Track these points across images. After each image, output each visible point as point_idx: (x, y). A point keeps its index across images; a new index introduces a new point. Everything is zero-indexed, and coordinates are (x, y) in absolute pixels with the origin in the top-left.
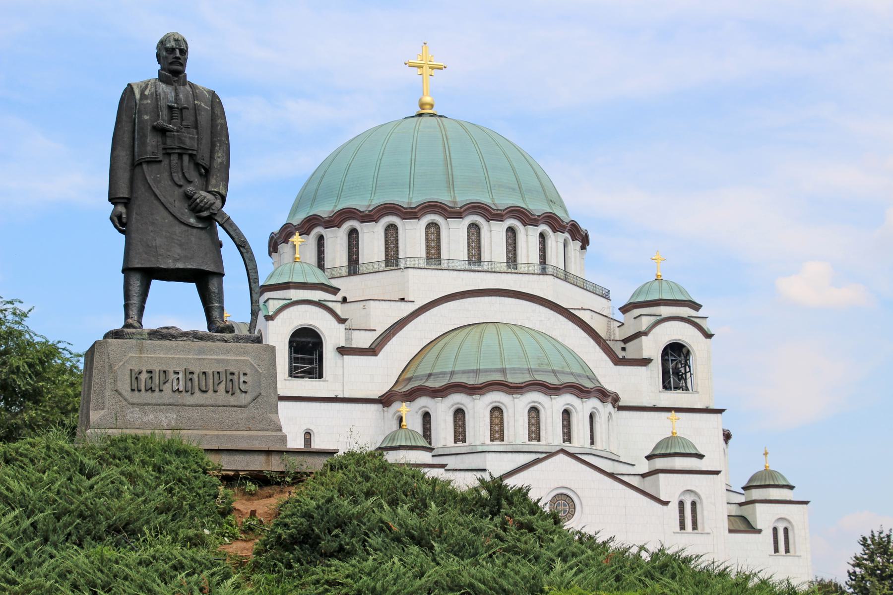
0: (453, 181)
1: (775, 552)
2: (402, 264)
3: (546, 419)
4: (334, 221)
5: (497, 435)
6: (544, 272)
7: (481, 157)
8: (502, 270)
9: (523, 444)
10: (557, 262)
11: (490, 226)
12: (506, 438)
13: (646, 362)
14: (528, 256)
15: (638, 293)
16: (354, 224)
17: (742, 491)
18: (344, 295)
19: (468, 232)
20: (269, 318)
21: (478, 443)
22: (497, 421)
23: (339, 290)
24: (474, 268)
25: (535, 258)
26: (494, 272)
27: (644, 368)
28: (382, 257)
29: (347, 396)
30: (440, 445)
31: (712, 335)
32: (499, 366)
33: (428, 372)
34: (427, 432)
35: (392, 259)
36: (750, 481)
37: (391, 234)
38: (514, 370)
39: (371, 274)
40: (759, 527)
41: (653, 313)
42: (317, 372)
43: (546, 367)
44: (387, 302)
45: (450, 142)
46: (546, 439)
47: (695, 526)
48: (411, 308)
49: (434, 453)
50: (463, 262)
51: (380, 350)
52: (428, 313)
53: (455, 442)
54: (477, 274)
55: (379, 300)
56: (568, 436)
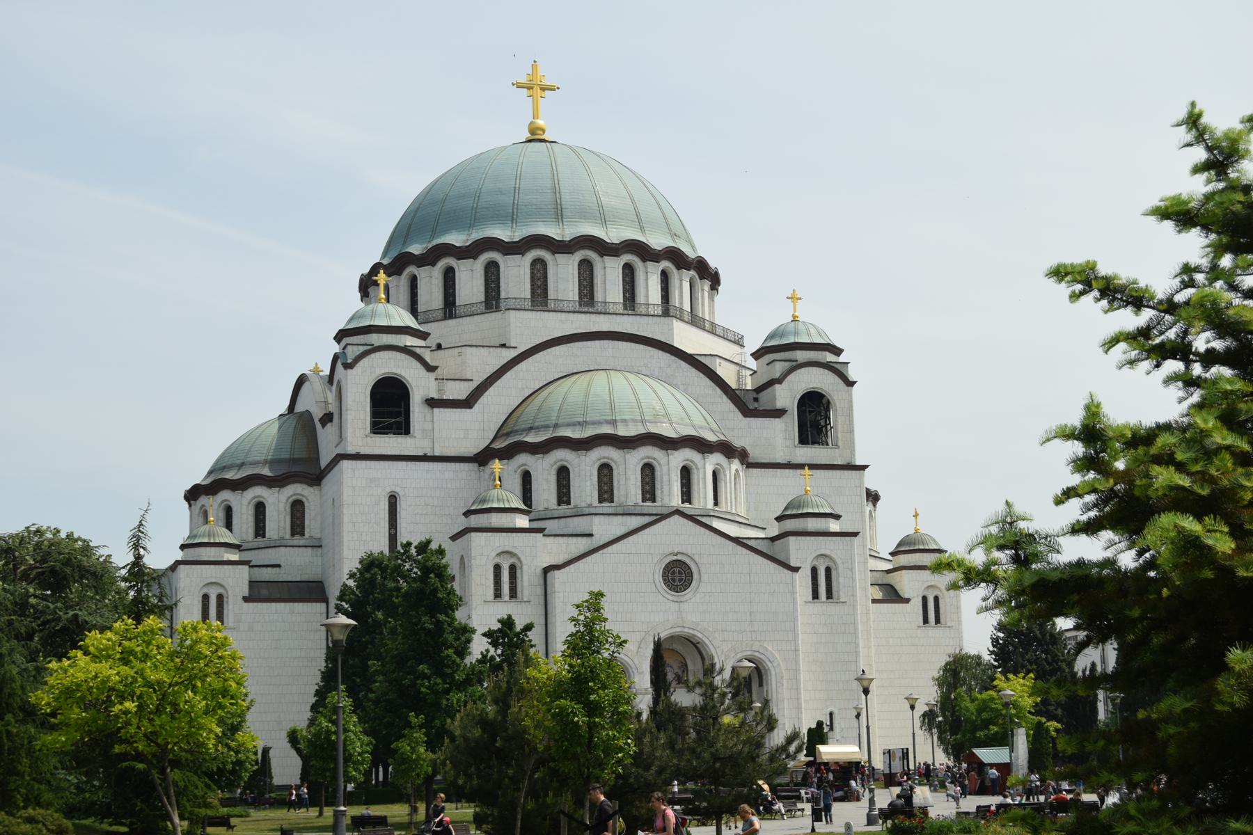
1: (924, 623)
2: (502, 307)
3: (661, 475)
4: (429, 258)
5: (606, 496)
6: (666, 313)
8: (617, 312)
9: (636, 505)
10: (681, 303)
11: (603, 261)
12: (616, 499)
13: (779, 413)
14: (647, 296)
15: (772, 336)
16: (451, 261)
17: (890, 558)
18: (438, 341)
19: (579, 269)
20: (348, 366)
21: (584, 505)
23: (429, 334)
24: (585, 309)
25: (655, 296)
26: (609, 314)
28: (483, 299)
29: (437, 453)
30: (541, 508)
31: (855, 382)
32: (610, 418)
33: (529, 426)
34: (527, 496)
35: (493, 299)
36: (899, 545)
37: (492, 273)
38: (625, 421)
39: (468, 318)
40: (906, 596)
41: (788, 358)
44: (486, 348)
45: (558, 168)
46: (662, 499)
48: (512, 354)
49: (533, 515)
50: (572, 303)
52: (530, 359)
53: (559, 505)
54: (588, 315)
55: (476, 346)
56: (687, 496)
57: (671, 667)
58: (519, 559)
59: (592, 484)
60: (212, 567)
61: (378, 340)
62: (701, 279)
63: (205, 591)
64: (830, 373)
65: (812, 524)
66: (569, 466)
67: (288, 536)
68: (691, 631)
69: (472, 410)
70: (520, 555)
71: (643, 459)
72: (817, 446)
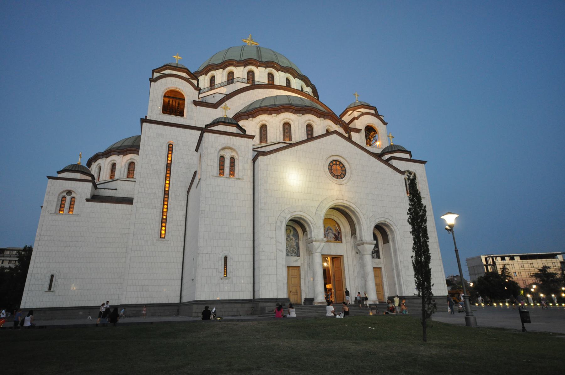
0: (261, 57)
22: (287, 131)
27: (358, 133)
31: (387, 123)
42: (181, 113)
52: (247, 92)
53: (260, 143)
57: (331, 230)
58: (237, 153)
59: (280, 131)
60: (70, 182)
63: (65, 194)
64: (377, 119)
67: (125, 177)
68: (348, 203)
69: (216, 109)
70: (237, 150)
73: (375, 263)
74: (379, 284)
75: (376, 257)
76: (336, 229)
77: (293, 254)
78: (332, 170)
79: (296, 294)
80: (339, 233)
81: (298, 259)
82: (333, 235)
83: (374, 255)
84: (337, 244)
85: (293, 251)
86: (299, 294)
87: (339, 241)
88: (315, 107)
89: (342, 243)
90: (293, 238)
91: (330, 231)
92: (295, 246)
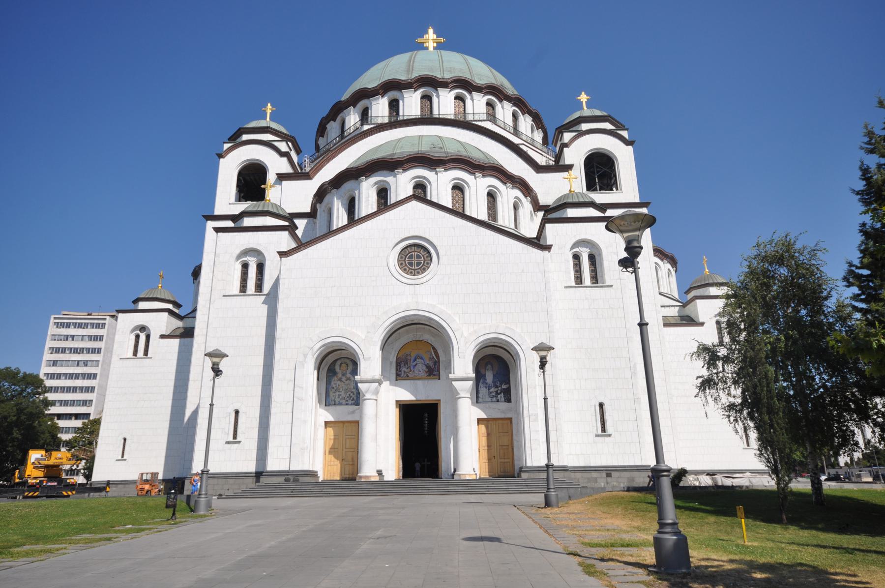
0: (413, 69)
7: (440, 55)
13: (568, 168)
40: (701, 320)
43: (437, 150)
47: (595, 278)
51: (315, 174)
57: (422, 358)
61: (245, 137)
62: (523, 115)
65: (571, 213)
66: (355, 196)
71: (414, 178)
72: (602, 191)
73: (499, 410)
74: (508, 446)
75: (503, 400)
76: (431, 357)
77: (350, 402)
78: (407, 262)
79: (351, 463)
80: (437, 363)
81: (357, 409)
82: (424, 368)
83: (499, 396)
84: (430, 381)
85: (350, 397)
86: (356, 463)
87: (434, 377)
88: (441, 150)
89: (439, 379)
90: (351, 376)
91: (419, 361)
92: (354, 388)
